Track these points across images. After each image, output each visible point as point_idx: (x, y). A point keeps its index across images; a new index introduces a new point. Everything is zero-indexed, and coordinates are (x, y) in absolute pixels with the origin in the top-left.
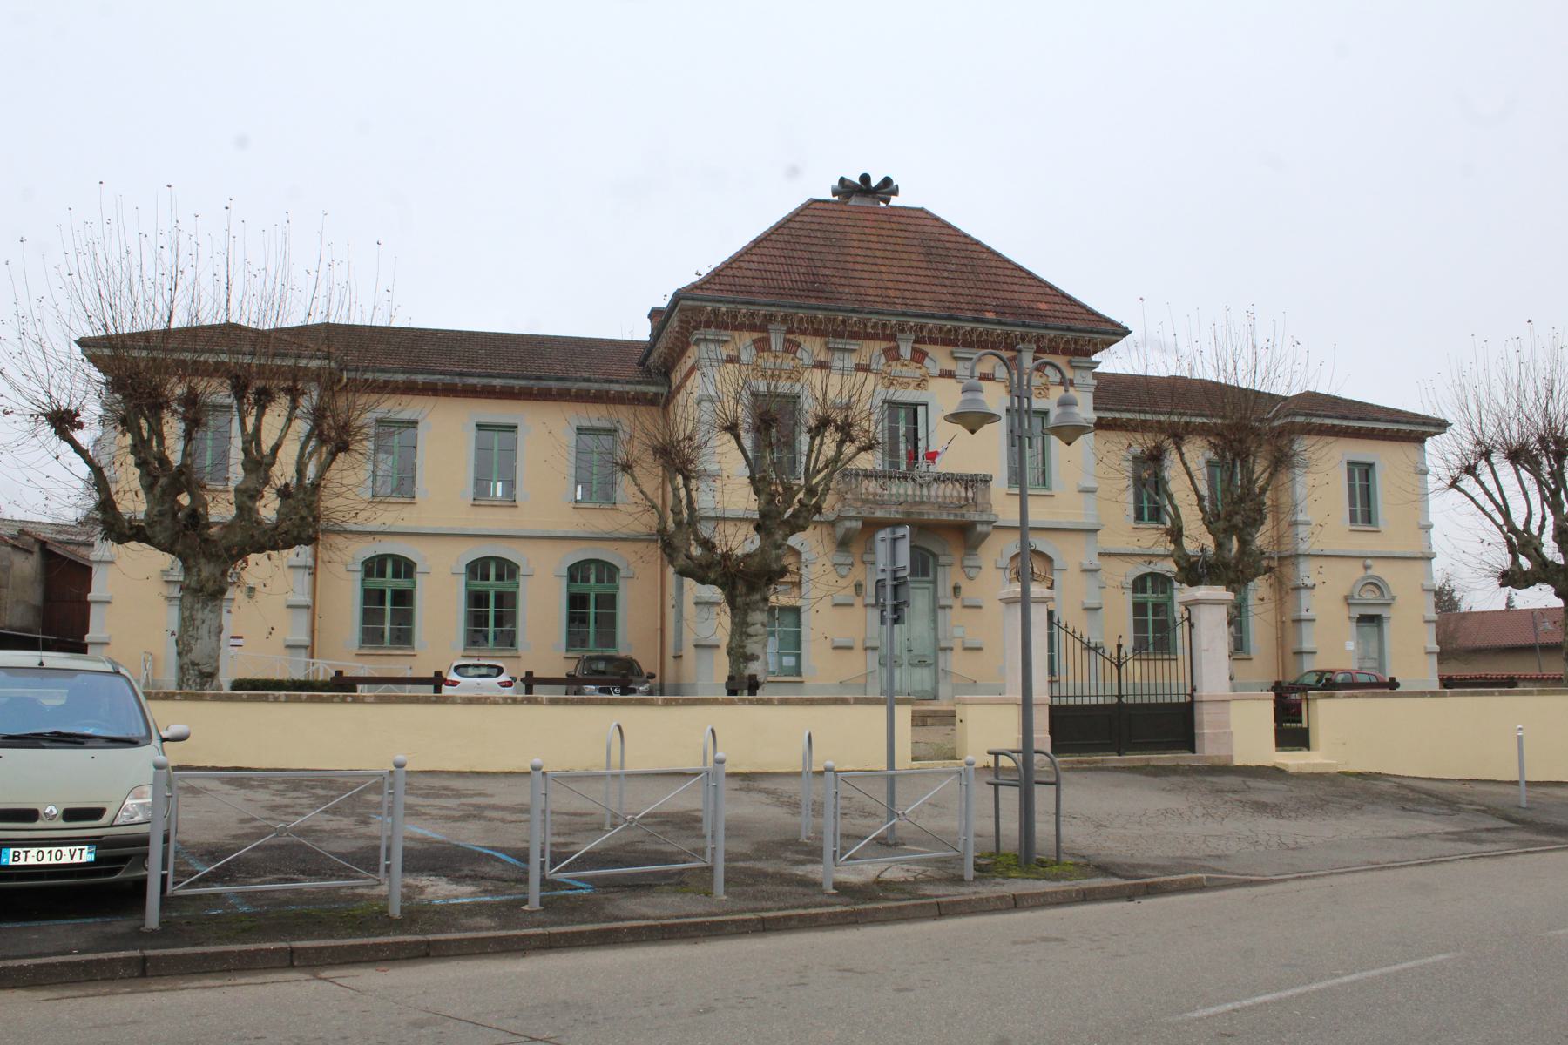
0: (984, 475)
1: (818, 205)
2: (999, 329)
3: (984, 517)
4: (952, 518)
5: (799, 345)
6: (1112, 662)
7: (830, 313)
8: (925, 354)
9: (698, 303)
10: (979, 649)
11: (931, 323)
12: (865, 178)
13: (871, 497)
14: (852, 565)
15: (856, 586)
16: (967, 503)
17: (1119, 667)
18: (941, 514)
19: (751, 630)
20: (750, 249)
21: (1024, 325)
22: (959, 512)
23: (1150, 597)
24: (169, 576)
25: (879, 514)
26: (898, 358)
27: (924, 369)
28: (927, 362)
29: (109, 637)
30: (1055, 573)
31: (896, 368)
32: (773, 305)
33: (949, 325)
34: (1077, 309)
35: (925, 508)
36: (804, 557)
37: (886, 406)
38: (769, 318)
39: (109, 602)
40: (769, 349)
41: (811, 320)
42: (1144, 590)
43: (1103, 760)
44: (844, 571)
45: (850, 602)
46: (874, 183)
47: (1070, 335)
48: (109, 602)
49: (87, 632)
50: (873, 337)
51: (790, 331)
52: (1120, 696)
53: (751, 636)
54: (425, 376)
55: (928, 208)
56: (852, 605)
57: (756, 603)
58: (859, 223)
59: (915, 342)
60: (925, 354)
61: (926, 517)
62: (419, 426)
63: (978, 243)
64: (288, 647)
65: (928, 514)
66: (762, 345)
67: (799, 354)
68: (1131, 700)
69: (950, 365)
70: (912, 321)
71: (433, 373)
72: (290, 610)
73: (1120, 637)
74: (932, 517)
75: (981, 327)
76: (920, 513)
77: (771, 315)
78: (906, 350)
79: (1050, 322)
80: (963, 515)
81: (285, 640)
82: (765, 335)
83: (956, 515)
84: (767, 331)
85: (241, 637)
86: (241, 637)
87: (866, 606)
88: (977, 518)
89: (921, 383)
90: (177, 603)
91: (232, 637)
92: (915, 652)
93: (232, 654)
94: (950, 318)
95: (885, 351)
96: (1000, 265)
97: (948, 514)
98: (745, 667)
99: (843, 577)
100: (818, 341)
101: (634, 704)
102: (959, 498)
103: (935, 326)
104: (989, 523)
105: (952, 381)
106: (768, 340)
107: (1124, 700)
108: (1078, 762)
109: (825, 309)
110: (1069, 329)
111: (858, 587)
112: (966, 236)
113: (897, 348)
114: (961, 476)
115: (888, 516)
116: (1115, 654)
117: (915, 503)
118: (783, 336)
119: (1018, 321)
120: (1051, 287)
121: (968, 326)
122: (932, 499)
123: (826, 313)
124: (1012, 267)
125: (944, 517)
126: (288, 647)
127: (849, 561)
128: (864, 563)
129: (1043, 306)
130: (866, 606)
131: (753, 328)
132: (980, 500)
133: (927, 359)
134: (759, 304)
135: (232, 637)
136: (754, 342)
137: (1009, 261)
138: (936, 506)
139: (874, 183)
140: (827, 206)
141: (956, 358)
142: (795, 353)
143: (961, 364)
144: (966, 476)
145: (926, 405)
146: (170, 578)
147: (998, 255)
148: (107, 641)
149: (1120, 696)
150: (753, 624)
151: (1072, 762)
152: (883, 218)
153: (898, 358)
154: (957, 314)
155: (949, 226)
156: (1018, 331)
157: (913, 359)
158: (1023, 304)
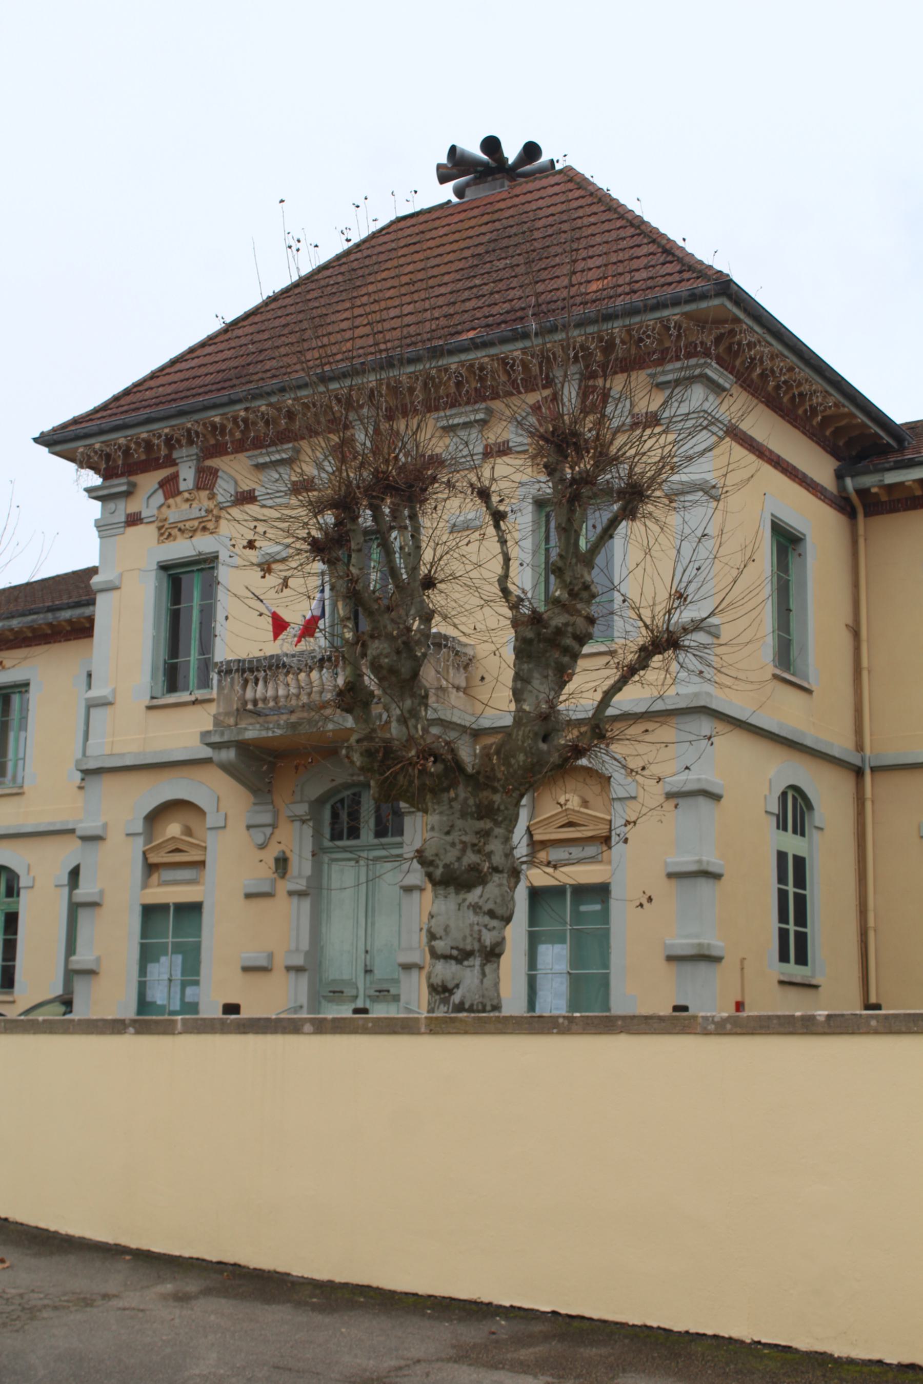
1: (402, 224)
12: (491, 145)
13: (250, 706)
14: (274, 826)
15: (277, 860)
18: (345, 720)
38: (171, 443)
45: (266, 888)
46: (511, 152)
54: (20, 619)
62: (32, 688)
66: (170, 487)
71: (32, 612)
92: (378, 974)
106: (175, 477)
111: (282, 863)
115: (264, 734)
122: (282, 702)
123: (221, 411)
127: (267, 818)
136: (162, 485)
139: (511, 152)
142: (211, 488)
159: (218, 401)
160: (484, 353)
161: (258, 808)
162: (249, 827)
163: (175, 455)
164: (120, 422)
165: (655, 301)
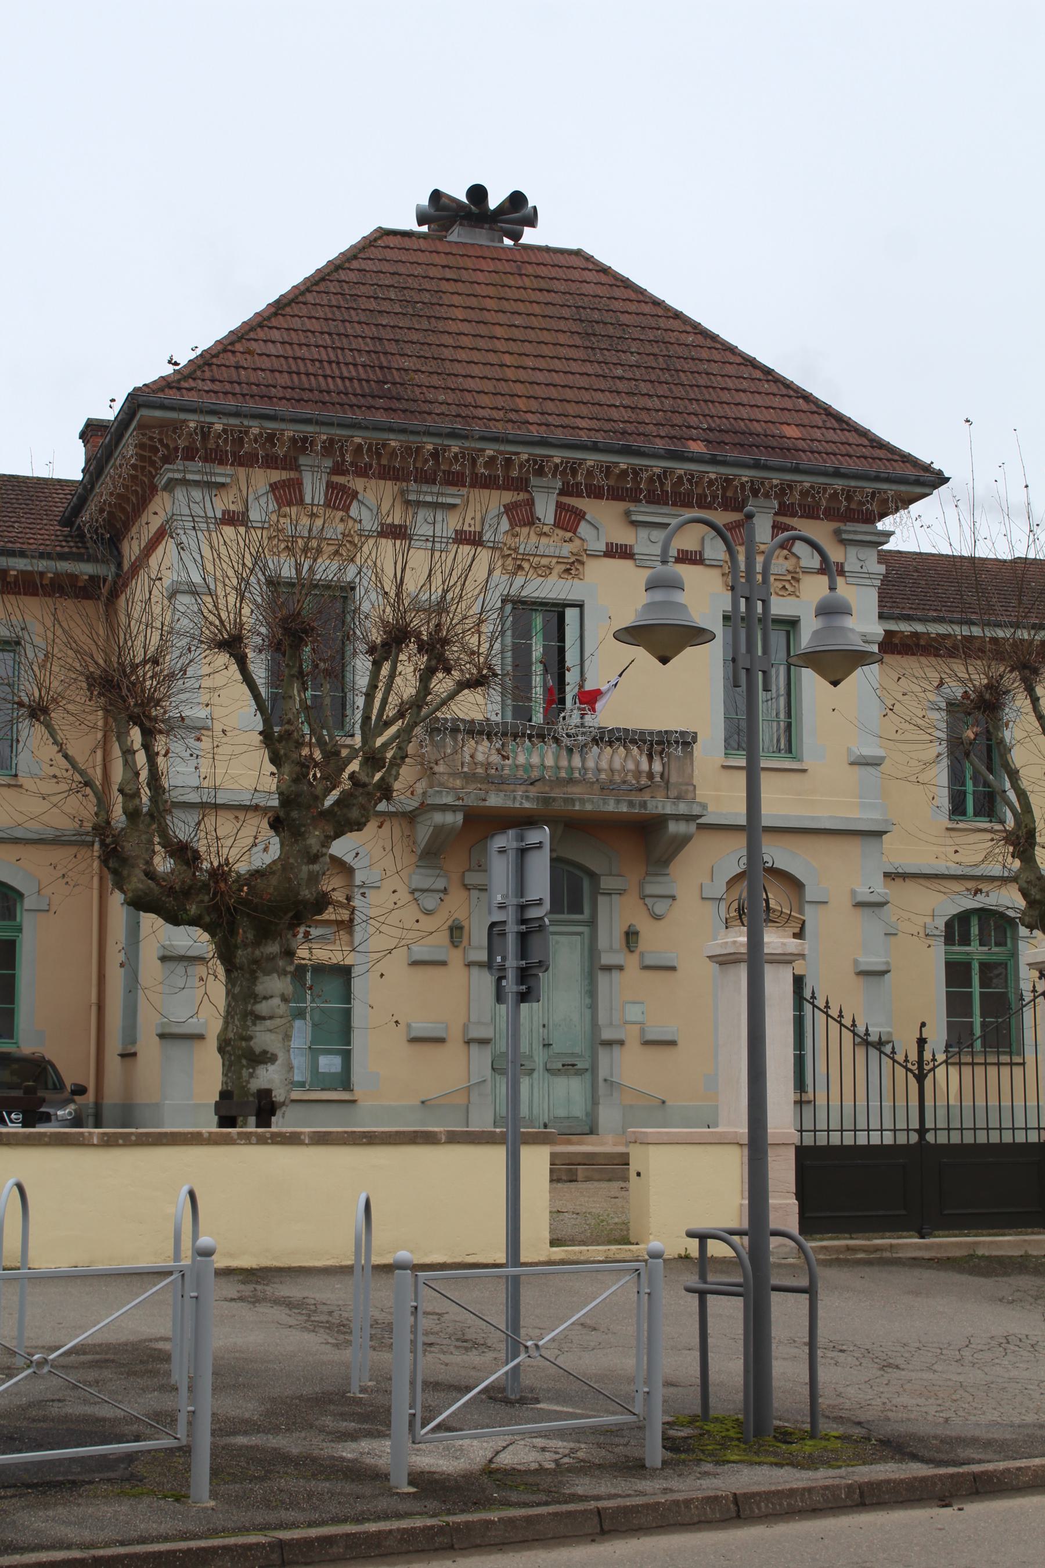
0: (683, 733)
2: (712, 472)
3: (682, 808)
4: (624, 808)
5: (355, 495)
6: (908, 1070)
7: (412, 438)
8: (580, 516)
9: (173, 415)
10: (672, 1043)
11: (591, 459)
12: (478, 193)
16: (650, 783)
17: (921, 1078)
19: (263, 1008)
20: (269, 318)
21: (757, 465)
22: (637, 798)
23: (976, 952)
25: (495, 800)
26: (531, 521)
27: (577, 542)
28: (583, 529)
30: (807, 908)
31: (528, 540)
32: (308, 421)
33: (624, 462)
34: (852, 438)
35: (576, 791)
36: (359, 878)
37: (509, 607)
38: (302, 445)
40: (301, 502)
41: (376, 450)
42: (965, 941)
43: (891, 1246)
44: (430, 902)
47: (839, 484)
50: (488, 483)
51: (338, 469)
52: (922, 1131)
53: (264, 1018)
55: (589, 250)
56: (443, 963)
57: (272, 958)
58: (465, 275)
59: (562, 493)
60: (580, 516)
61: (577, 808)
63: (678, 315)
65: (582, 801)
67: (354, 511)
68: (942, 1139)
69: (624, 536)
70: (558, 456)
73: (923, 1025)
74: (589, 807)
75: (681, 468)
76: (566, 800)
77: (305, 440)
78: (545, 508)
79: (805, 460)
80: (644, 805)
82: (293, 475)
83: (631, 804)
84: (297, 468)
87: (469, 965)
88: (669, 810)
89: (572, 568)
92: (556, 1048)
94: (627, 451)
95: (509, 509)
96: (716, 356)
97: (618, 802)
98: (251, 1075)
99: (428, 913)
100: (388, 489)
101: (48, 1144)
102: (638, 773)
103: (599, 465)
104: (689, 818)
105: (628, 564)
106: (297, 485)
107: (930, 1137)
108: (848, 1248)
109: (403, 431)
110: (837, 474)
111: (456, 932)
112: (657, 303)
113: (531, 503)
114: (642, 733)
115: (509, 804)
116: (913, 1056)
117: (559, 782)
118: (325, 478)
119: (747, 457)
120: (807, 397)
121: (658, 466)
123: (402, 437)
124: (739, 360)
125: (611, 807)
127: (440, 884)
128: (467, 887)
129: (791, 432)
130: (469, 965)
131: (271, 462)
132: (674, 779)
133: (583, 524)
134: (283, 420)
136: (274, 487)
137: (732, 350)
138: (596, 787)
140: (407, 243)
141: (635, 524)
142: (347, 509)
143: (643, 533)
144: (651, 733)
145: (581, 606)
147: (714, 338)
149: (922, 1131)
150: (265, 998)
151: (837, 1250)
152: (508, 267)
153: (531, 521)
154: (636, 442)
155: (626, 284)
156: (746, 475)
157: (558, 524)
158: (757, 428)
159: (411, 428)
160: (714, 470)
161: (422, 871)
162: (412, 892)
163: (302, 460)
164: (272, 413)
165: (886, 475)
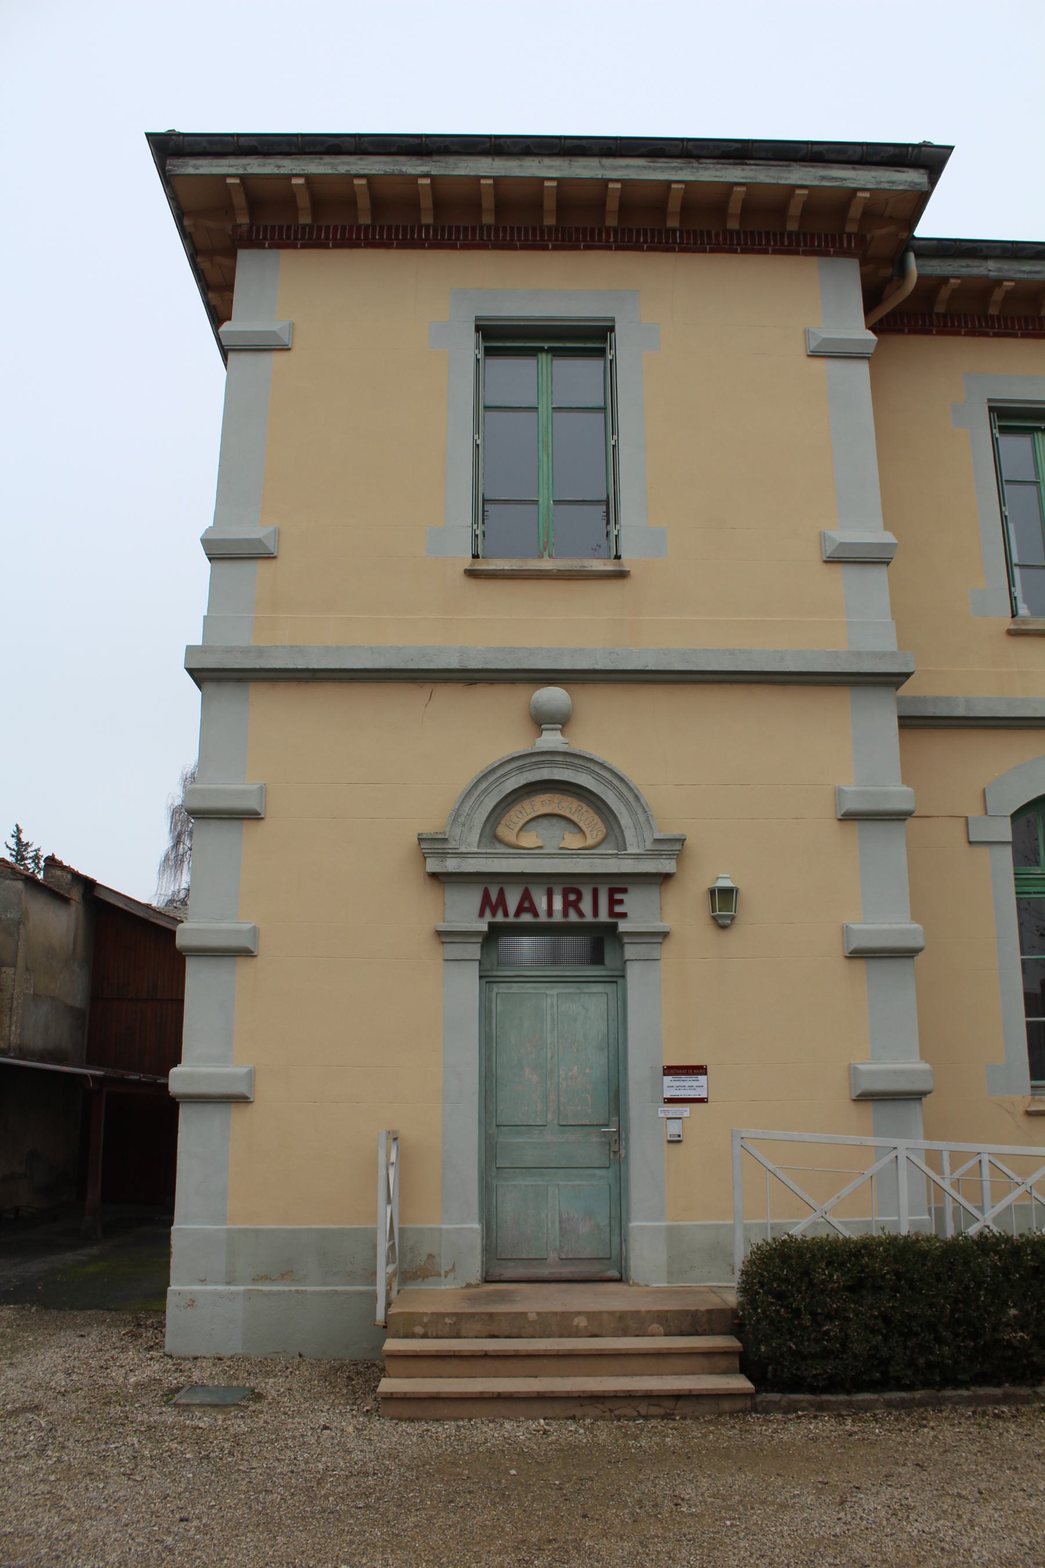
24: (443, 855)
29: (251, 1076)
39: (246, 953)
48: (246, 953)
49: (177, 1060)
64: (866, 1098)
72: (859, 965)
81: (853, 1072)
85: (699, 1070)
86: (699, 1070)
90: (474, 951)
91: (670, 1070)
93: (674, 1128)
126: (866, 1098)
135: (670, 1070)
146: (451, 865)
148: (240, 1089)
